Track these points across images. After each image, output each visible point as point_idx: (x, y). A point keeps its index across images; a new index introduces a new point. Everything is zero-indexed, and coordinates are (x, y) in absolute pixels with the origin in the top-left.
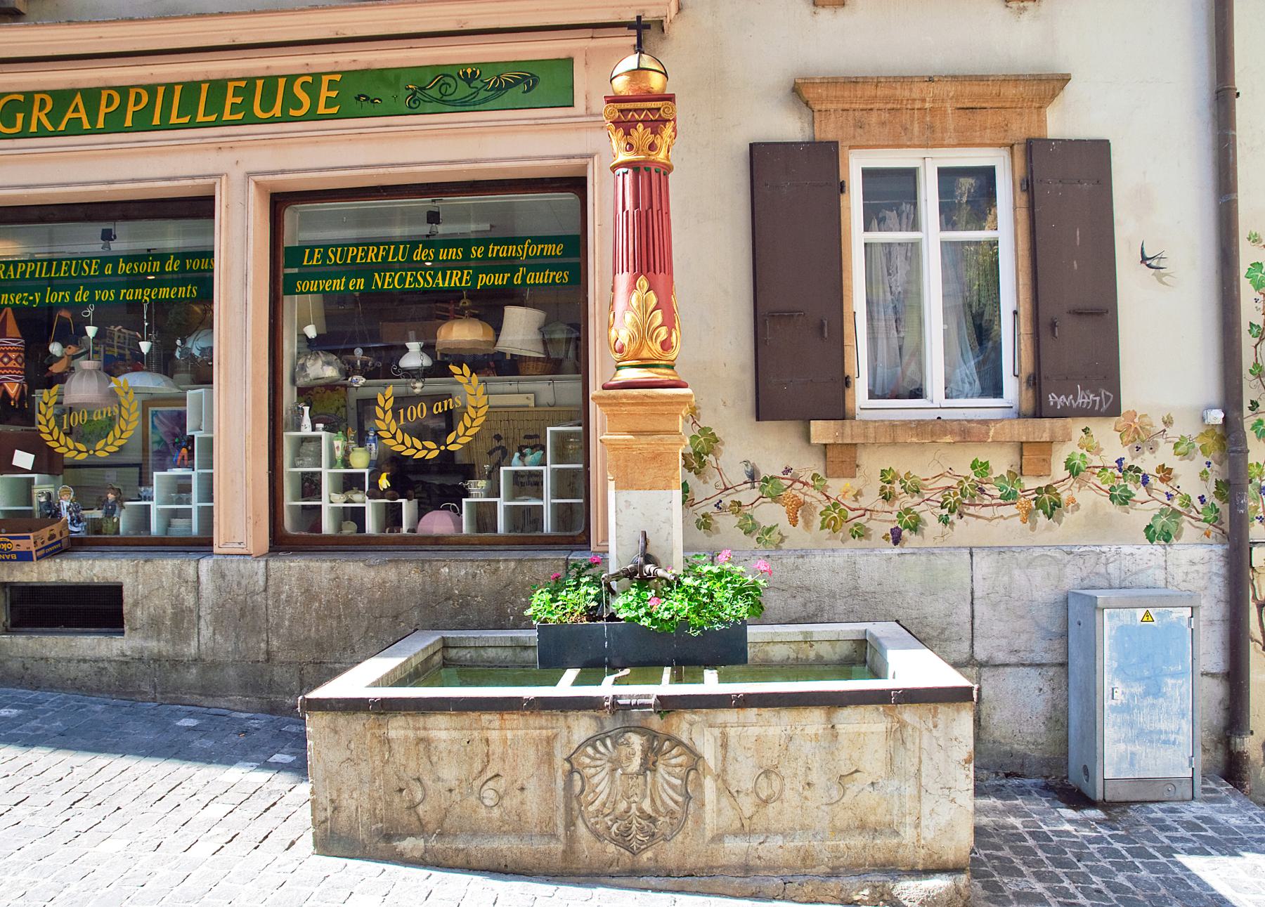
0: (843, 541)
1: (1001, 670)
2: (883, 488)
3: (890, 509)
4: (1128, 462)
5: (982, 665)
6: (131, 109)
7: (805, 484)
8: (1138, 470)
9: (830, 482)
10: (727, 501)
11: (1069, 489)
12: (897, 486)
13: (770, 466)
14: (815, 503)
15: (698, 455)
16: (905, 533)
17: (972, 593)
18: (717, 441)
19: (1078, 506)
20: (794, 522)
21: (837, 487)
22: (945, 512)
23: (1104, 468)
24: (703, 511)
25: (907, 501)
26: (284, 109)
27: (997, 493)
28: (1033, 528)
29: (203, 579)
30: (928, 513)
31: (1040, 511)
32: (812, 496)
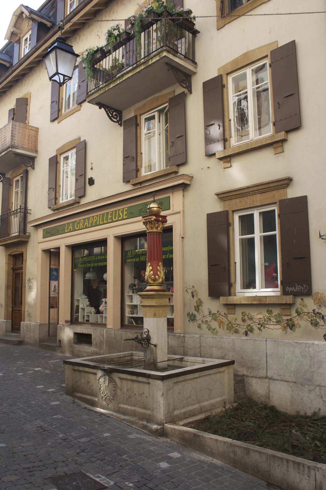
0: (232, 334)
1: (276, 381)
2: (242, 318)
3: (244, 325)
4: (317, 311)
5: (270, 379)
6: (94, 221)
7: (222, 316)
8: (320, 314)
9: (229, 315)
10: (204, 320)
11: (297, 320)
12: (246, 317)
13: (214, 311)
14: (225, 322)
15: (198, 306)
16: (249, 332)
17: (266, 354)
18: (202, 302)
19: (300, 326)
20: (220, 327)
21: (230, 317)
22: (260, 326)
23: (309, 313)
24: (199, 323)
25: (249, 322)
26: (118, 218)
27: (275, 321)
28: (286, 333)
29: (104, 334)
30: (255, 326)
31: (288, 327)
32: (224, 320)
